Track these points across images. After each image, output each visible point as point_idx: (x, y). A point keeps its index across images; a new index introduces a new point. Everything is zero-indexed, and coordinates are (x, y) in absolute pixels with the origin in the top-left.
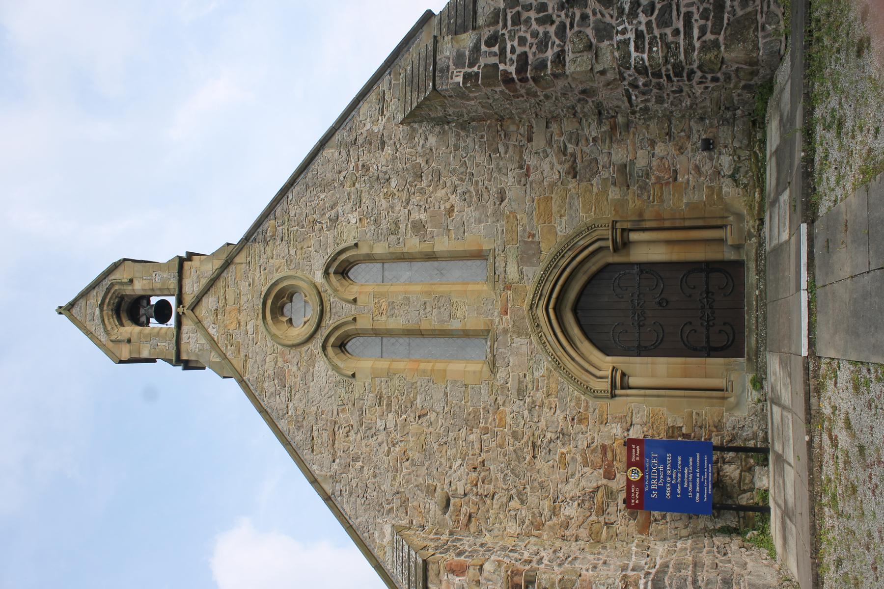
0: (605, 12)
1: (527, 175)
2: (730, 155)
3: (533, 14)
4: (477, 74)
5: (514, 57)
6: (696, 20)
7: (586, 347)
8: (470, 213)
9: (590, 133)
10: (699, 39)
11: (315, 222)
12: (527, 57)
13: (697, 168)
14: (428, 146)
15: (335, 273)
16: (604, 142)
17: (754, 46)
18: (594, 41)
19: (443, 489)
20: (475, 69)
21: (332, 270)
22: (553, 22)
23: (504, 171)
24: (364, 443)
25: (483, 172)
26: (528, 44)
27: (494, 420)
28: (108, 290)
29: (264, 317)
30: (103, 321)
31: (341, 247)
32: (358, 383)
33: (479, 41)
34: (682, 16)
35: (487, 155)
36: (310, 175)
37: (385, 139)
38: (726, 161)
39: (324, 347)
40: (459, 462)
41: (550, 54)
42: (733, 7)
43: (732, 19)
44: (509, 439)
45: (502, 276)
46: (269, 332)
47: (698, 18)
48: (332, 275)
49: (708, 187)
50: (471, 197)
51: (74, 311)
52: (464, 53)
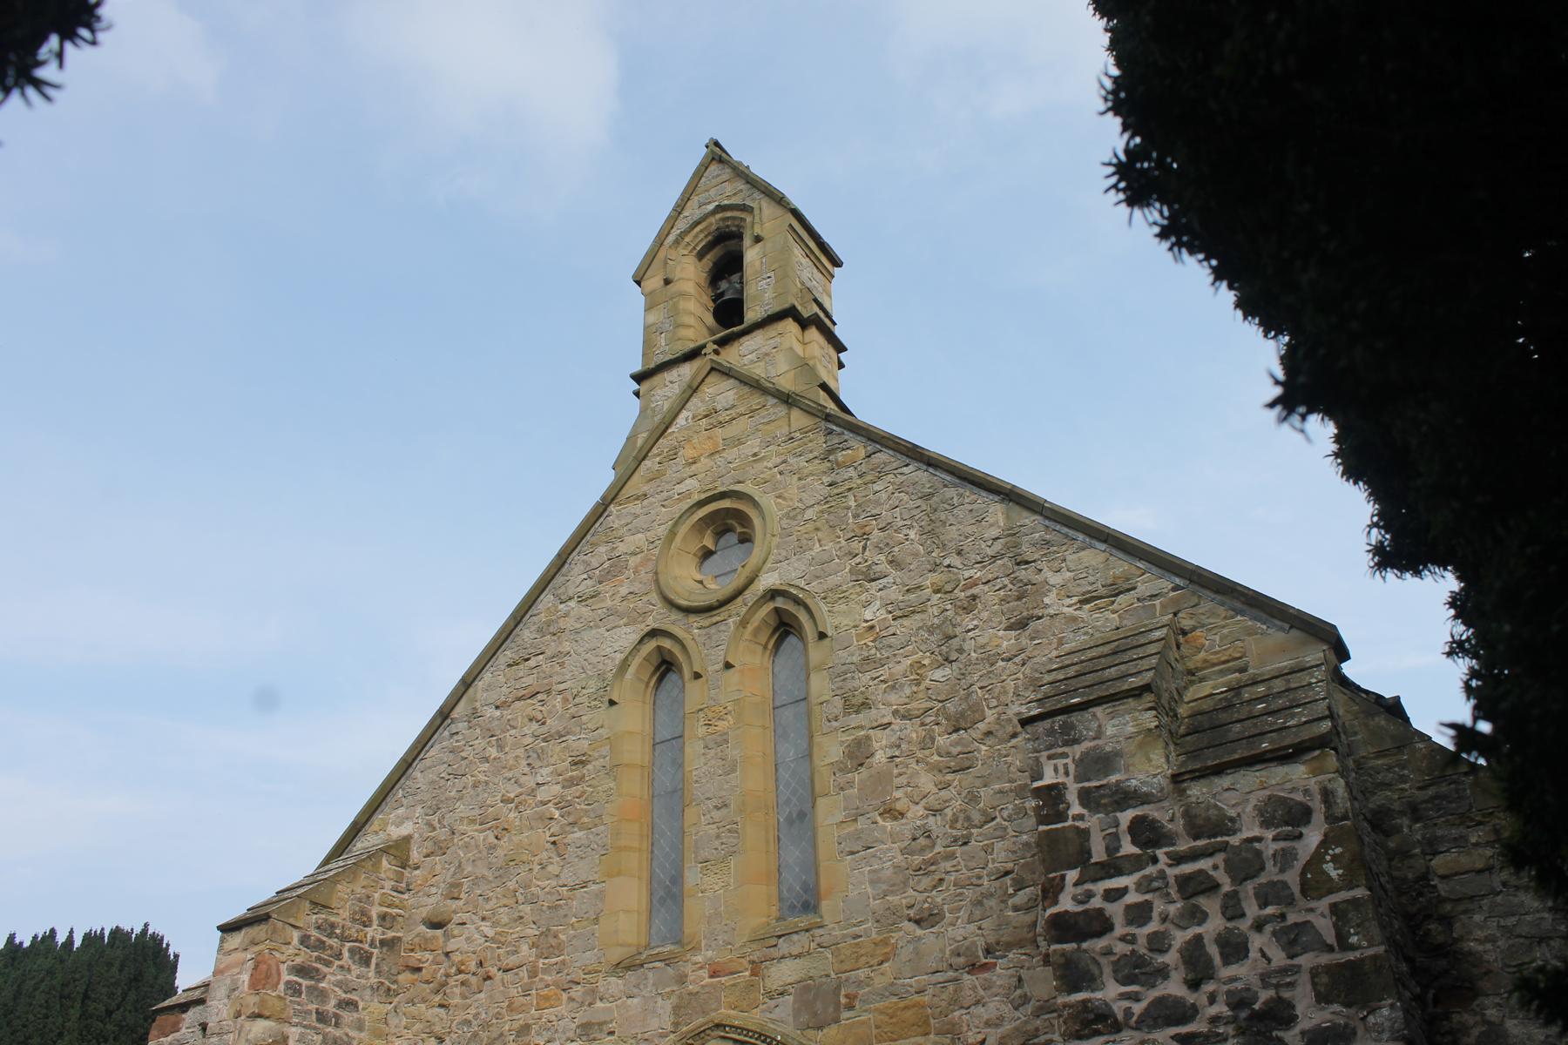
1: (973, 968)
4: (1061, 817)
5: (1096, 902)
8: (890, 856)
11: (865, 536)
12: (1100, 934)
15: (777, 610)
19: (455, 912)
20: (1076, 809)
21: (780, 603)
22: (1194, 985)
23: (978, 913)
24: (520, 752)
26: (1132, 930)
27: (547, 986)
28: (744, 208)
29: (701, 504)
30: (697, 223)
32: (603, 714)
33: (1145, 799)
35: (1010, 865)
36: (951, 492)
37: (1033, 625)
39: (654, 633)
40: (490, 933)
41: (1110, 992)
44: (521, 1019)
45: (774, 952)
46: (676, 524)
48: (771, 606)
50: (922, 850)
51: (714, 168)
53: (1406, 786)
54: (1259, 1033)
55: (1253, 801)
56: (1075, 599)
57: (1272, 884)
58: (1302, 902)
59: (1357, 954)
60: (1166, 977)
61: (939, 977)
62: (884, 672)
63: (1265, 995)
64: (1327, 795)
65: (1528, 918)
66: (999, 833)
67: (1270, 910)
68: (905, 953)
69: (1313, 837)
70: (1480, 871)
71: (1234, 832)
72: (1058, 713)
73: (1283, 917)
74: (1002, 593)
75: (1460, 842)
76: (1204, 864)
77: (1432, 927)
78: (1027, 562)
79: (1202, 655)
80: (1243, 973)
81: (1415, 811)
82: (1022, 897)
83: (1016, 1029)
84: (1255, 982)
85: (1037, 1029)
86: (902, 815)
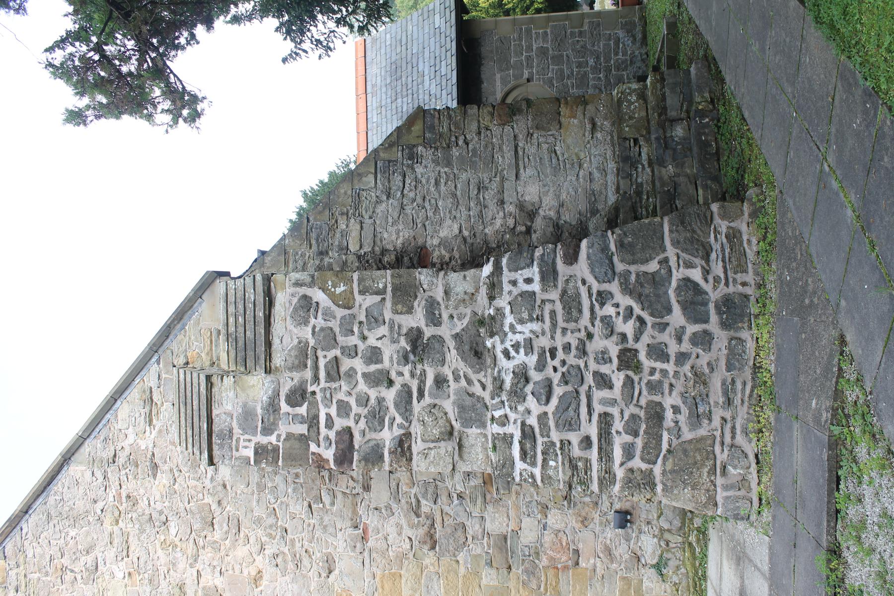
0: (474, 377)
1: (364, 538)
2: (654, 536)
3: (358, 364)
4: (276, 449)
5: (332, 435)
6: (617, 432)
9: (454, 486)
10: (622, 464)
13: (608, 551)
14: (219, 478)
16: (473, 501)
17: (709, 498)
18: (457, 426)
20: (273, 439)
22: (391, 383)
23: (331, 530)
25: (300, 528)
26: (352, 415)
34: (595, 418)
35: (306, 504)
37: (156, 460)
38: (649, 545)
41: (387, 436)
42: (677, 422)
43: (675, 442)
47: (621, 430)
49: (623, 578)
50: (285, 561)
52: (255, 409)
53: (308, 254)
54: (423, 351)
55: (291, 327)
56: (148, 428)
57: (341, 325)
58: (354, 311)
59: (389, 285)
60: (384, 399)
61: (367, 562)
62: (163, 569)
63: (403, 343)
64: (298, 284)
65: (390, 211)
66: (284, 507)
67: (356, 329)
68: (349, 583)
69: (319, 296)
70: (362, 228)
71: (307, 343)
72: (209, 440)
73: (361, 323)
74: (130, 477)
75: (345, 234)
76: (322, 363)
77: (386, 259)
78: (115, 456)
79: (203, 355)
80: (389, 352)
81: (322, 253)
82: (326, 499)
83: (405, 516)
84: (395, 346)
85: (407, 502)
86: (259, 572)
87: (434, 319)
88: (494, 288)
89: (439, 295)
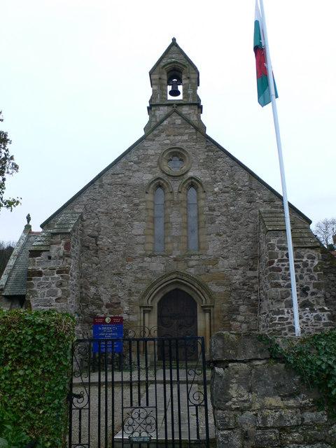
1: (235, 269)
7: (161, 295)
15: (192, 182)
18: (285, 300)
21: (193, 180)
29: (170, 149)
31: (204, 185)
39: (158, 178)
76: (299, 263)
87: (313, 294)
88: (323, 310)
89: (318, 295)
